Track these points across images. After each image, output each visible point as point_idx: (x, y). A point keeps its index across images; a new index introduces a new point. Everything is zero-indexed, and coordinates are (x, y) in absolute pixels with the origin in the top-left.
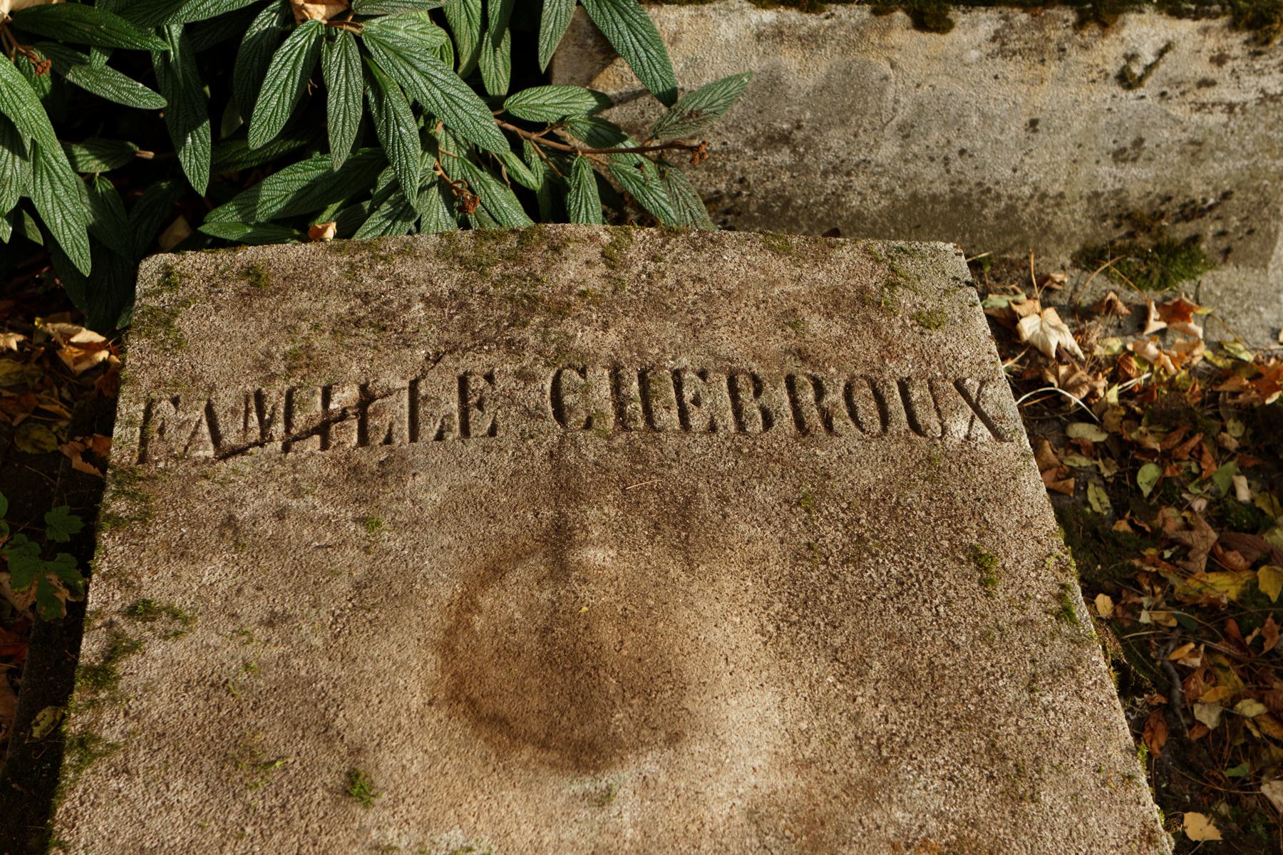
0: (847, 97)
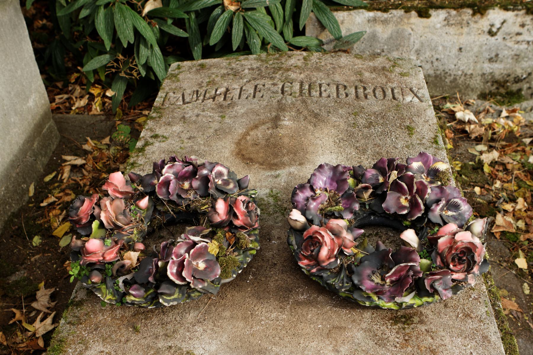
0: (398, 40)
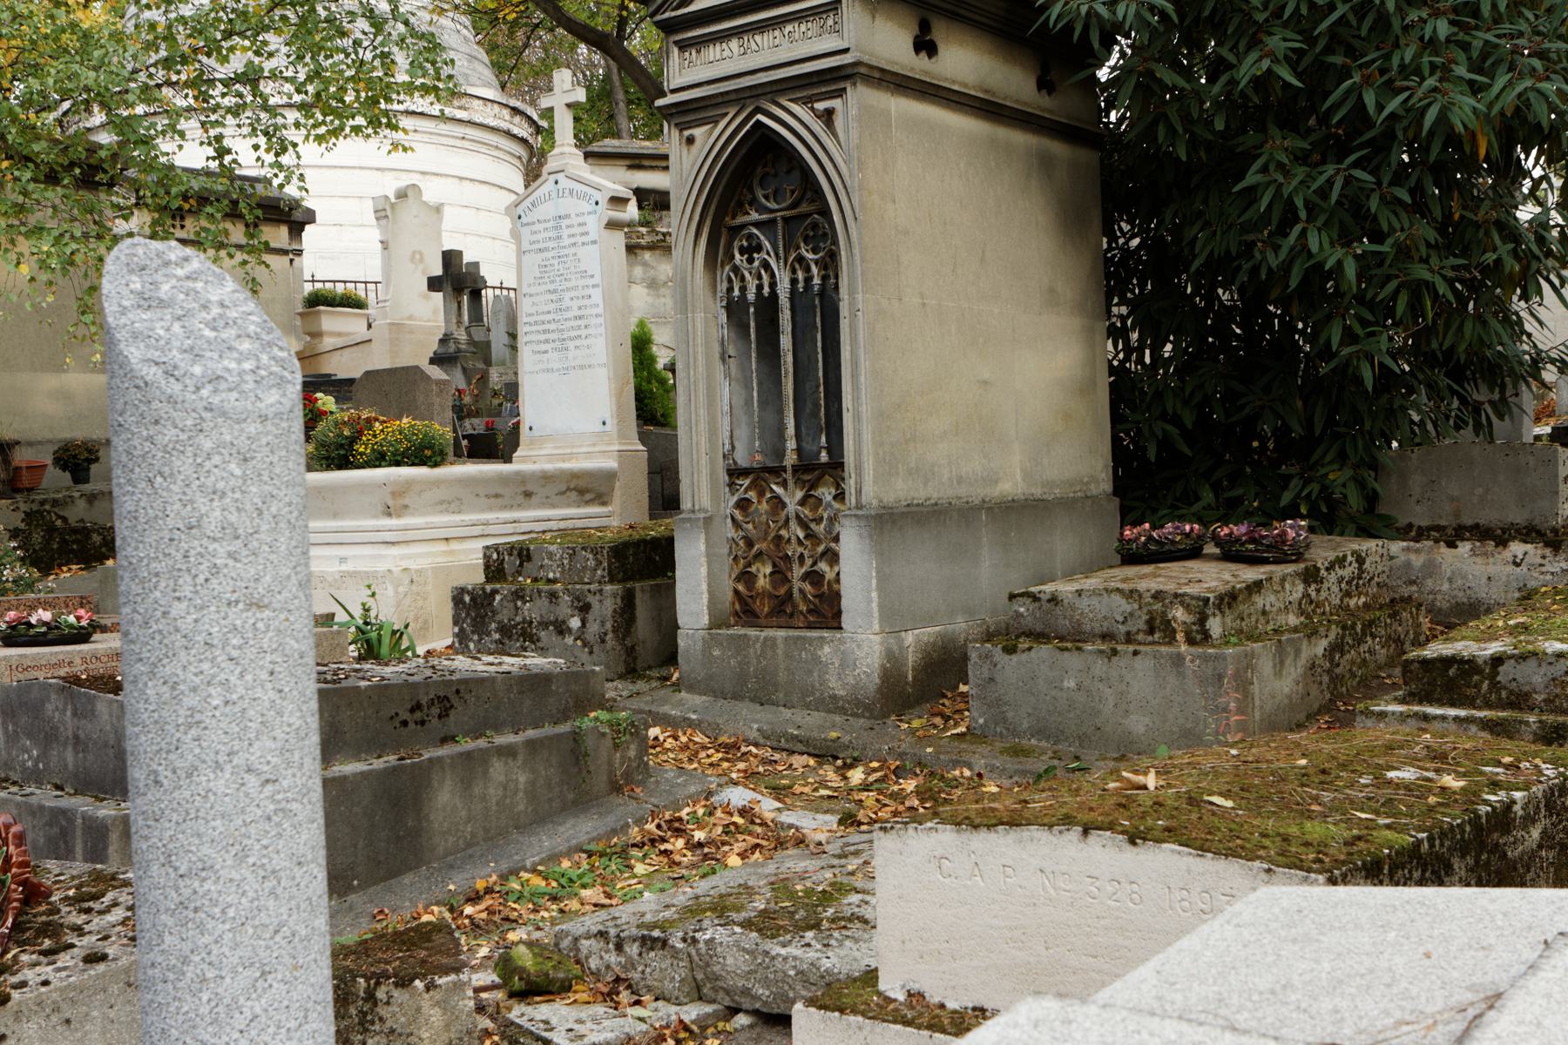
0: (1431, 569)
